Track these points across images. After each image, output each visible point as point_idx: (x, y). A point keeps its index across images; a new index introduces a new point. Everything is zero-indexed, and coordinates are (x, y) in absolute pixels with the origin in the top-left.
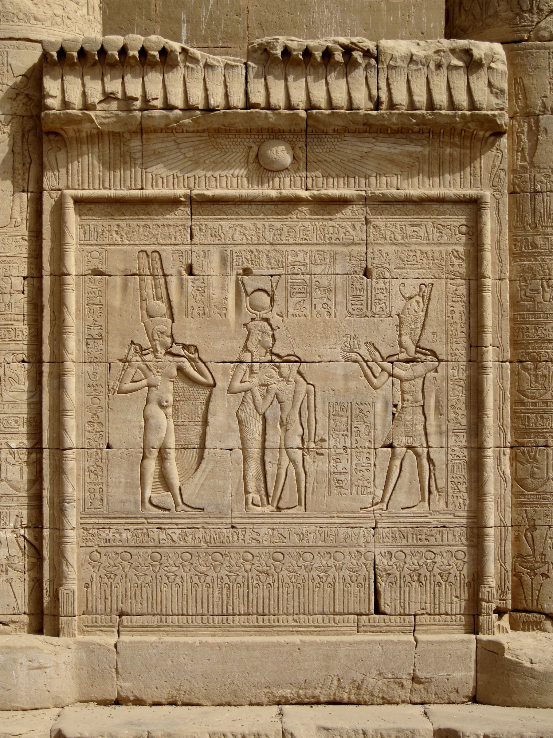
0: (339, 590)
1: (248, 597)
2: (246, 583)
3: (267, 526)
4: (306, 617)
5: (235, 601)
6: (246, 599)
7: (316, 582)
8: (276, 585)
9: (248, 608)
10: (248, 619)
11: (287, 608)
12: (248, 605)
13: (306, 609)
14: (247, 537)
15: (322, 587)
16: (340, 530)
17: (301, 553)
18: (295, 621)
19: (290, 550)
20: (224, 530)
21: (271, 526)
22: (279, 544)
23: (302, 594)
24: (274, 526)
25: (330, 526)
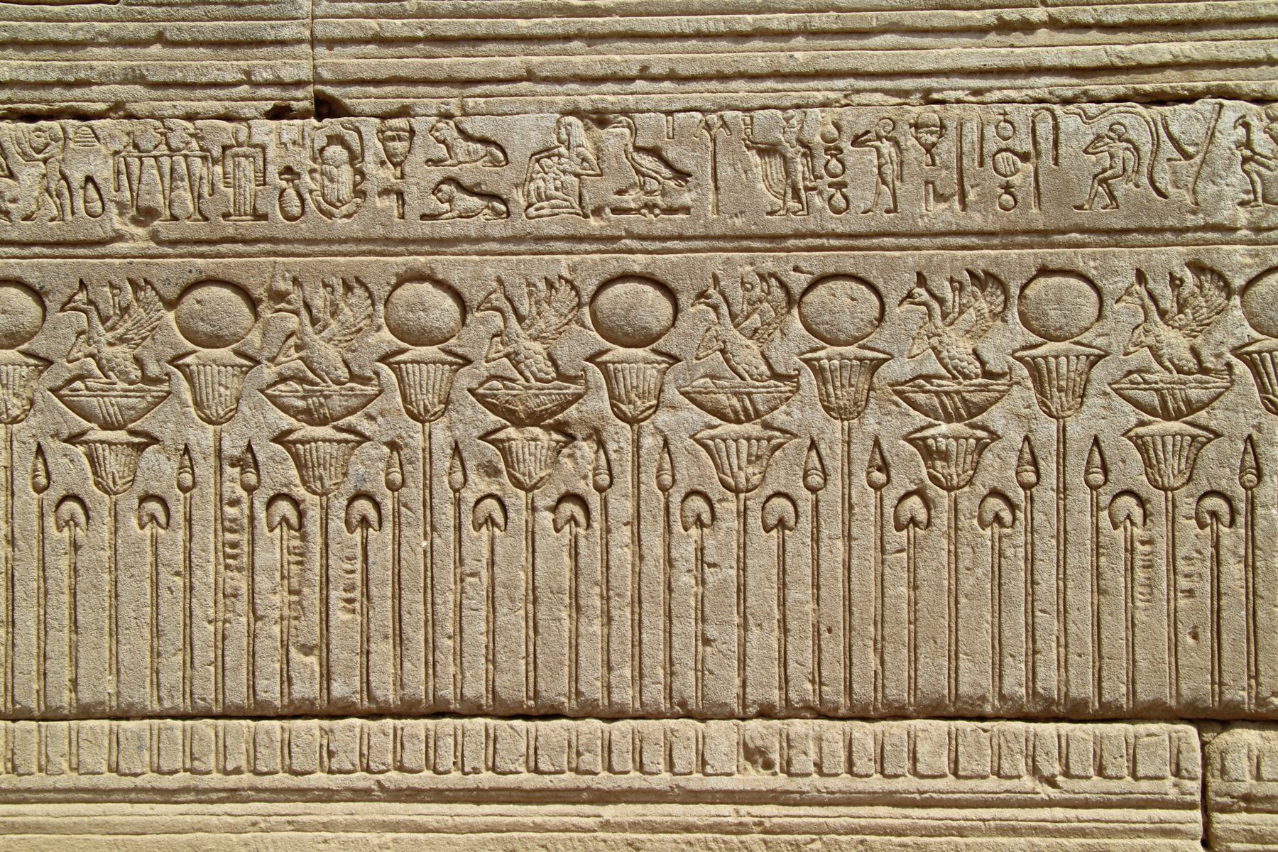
0: (1063, 537)
1: (430, 587)
2: (414, 493)
3: (563, 96)
4: (833, 730)
5: (339, 615)
6: (414, 601)
7: (901, 483)
8: (622, 507)
9: (432, 666)
10: (432, 743)
11: (701, 669)
12: (432, 646)
13: (834, 672)
14: (421, 175)
15: (942, 519)
16: (1070, 121)
17: (798, 282)
18: (754, 755)
19: (715, 261)
20: (264, 130)
21: (588, 98)
22: (638, 223)
23: (801, 569)
24: (608, 96)
25: (1000, 88)
